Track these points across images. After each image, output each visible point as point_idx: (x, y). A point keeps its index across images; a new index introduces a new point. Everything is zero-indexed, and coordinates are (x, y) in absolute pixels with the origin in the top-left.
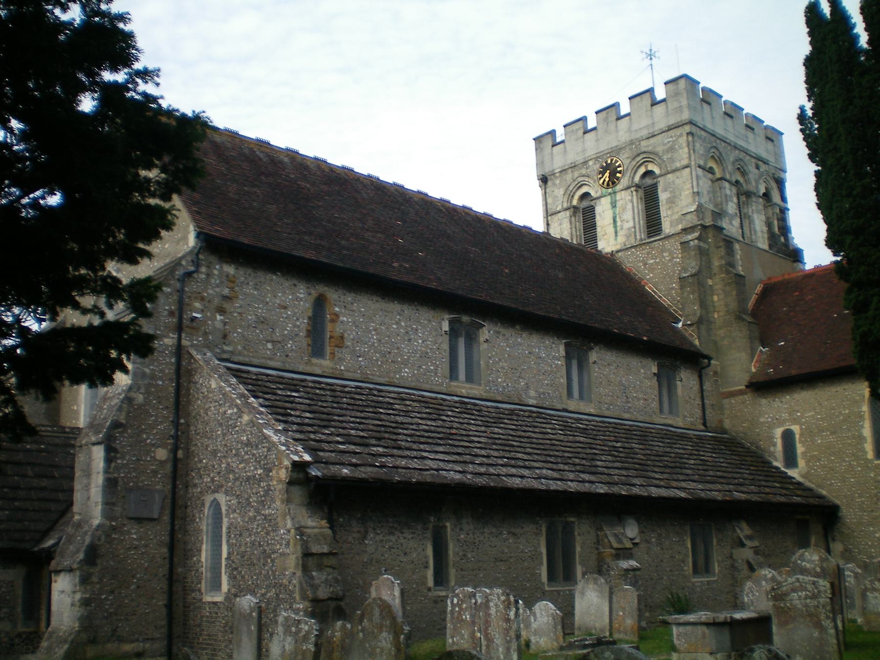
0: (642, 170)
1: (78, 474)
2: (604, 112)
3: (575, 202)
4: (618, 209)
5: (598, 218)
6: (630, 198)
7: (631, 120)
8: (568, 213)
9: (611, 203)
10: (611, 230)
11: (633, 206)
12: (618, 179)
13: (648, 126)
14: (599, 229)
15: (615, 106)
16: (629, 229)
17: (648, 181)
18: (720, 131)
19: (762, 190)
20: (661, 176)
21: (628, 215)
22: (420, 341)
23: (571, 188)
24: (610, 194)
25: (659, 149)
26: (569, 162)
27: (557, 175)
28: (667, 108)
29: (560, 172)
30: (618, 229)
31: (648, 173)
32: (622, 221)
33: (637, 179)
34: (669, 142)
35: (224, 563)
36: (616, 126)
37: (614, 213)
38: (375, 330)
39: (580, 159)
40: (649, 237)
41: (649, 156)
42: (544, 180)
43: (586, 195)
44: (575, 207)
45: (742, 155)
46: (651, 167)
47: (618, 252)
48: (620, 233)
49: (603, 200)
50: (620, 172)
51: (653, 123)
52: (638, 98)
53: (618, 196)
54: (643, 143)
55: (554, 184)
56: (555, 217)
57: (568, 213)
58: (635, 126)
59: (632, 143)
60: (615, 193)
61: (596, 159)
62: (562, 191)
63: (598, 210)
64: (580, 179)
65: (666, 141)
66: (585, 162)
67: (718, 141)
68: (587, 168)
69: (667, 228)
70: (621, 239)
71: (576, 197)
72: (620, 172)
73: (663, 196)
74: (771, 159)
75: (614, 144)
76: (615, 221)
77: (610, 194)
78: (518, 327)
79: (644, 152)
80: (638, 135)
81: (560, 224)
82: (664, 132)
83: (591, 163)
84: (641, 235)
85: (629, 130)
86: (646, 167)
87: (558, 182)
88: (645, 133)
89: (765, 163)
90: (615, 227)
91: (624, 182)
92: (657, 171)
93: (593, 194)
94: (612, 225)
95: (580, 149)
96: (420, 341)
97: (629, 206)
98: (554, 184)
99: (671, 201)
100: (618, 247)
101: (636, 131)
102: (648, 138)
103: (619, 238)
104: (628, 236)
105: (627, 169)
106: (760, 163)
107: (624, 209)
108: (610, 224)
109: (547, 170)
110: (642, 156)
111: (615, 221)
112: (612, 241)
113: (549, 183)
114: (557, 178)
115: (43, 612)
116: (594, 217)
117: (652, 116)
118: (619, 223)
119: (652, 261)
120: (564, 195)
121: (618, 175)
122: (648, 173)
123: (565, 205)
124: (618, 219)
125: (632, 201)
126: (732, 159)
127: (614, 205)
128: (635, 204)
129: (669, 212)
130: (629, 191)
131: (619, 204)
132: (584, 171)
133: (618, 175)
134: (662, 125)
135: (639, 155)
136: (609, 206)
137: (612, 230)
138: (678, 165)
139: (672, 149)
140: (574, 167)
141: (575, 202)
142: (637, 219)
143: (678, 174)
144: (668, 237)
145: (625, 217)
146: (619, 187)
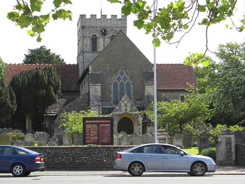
0: (112, 34)
8: (90, 39)
33: (110, 36)
39: (95, 26)
53: (105, 39)
54: (114, 28)
56: (86, 38)
57: (90, 39)
59: (111, 27)
66: (96, 27)
71: (92, 35)
83: (98, 28)
85: (110, 23)
87: (87, 29)
88: (115, 26)
91: (108, 36)
95: (95, 23)
98: (86, 29)
105: (109, 33)
109: (84, 25)
113: (84, 29)
114: (87, 28)
120: (89, 33)
127: (104, 41)
131: (106, 41)
132: (96, 29)
134: (120, 26)
140: (93, 27)
141: (91, 36)
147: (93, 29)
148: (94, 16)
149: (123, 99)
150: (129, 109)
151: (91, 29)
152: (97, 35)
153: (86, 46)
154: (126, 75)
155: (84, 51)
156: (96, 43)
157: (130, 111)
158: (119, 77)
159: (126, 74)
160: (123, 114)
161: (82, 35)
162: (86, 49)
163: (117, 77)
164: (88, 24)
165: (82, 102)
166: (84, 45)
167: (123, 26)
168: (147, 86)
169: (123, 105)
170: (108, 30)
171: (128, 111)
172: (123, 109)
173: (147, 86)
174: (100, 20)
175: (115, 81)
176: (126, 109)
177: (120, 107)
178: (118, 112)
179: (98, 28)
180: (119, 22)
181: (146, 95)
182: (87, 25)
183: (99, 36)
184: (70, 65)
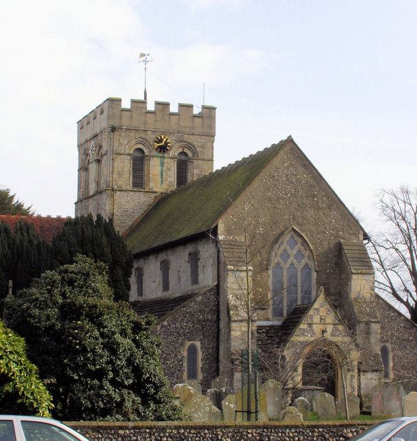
0: (181, 150)
3: (131, 152)
7: (179, 118)
8: (129, 157)
15: (167, 105)
17: (183, 158)
24: (161, 157)
25: (195, 143)
31: (183, 153)
33: (176, 154)
37: (162, 169)
41: (190, 146)
46: (186, 150)
49: (155, 159)
52: (185, 108)
53: (166, 160)
56: (120, 157)
58: (182, 124)
59: (179, 132)
60: (164, 157)
72: (169, 146)
76: (162, 175)
81: (123, 162)
83: (149, 133)
87: (123, 134)
88: (187, 130)
90: (162, 178)
91: (171, 153)
92: (190, 154)
98: (120, 135)
111: (162, 175)
112: (159, 186)
122: (183, 153)
127: (162, 165)
134: (198, 130)
136: (159, 164)
137: (160, 179)
141: (131, 152)
146: (166, 155)
147: (138, 136)
148: (140, 105)
149: (316, 306)
150: (330, 329)
152: (146, 151)
153: (120, 175)
154: (302, 248)
155: (115, 187)
156: (142, 170)
157: (333, 335)
158: (285, 250)
159: (302, 245)
160: (317, 342)
161: (112, 147)
162: (120, 183)
163: (280, 252)
164: (125, 123)
165: (200, 311)
166: (115, 172)
168: (354, 277)
169: (316, 319)
171: (328, 335)
172: (317, 328)
173: (354, 277)
174: (153, 115)
175: (276, 262)
176: (323, 332)
177: (310, 325)
178: (304, 335)
179: (149, 133)
180: (198, 121)
181: (352, 297)
182: (123, 124)
183: (150, 152)
184: (49, 217)
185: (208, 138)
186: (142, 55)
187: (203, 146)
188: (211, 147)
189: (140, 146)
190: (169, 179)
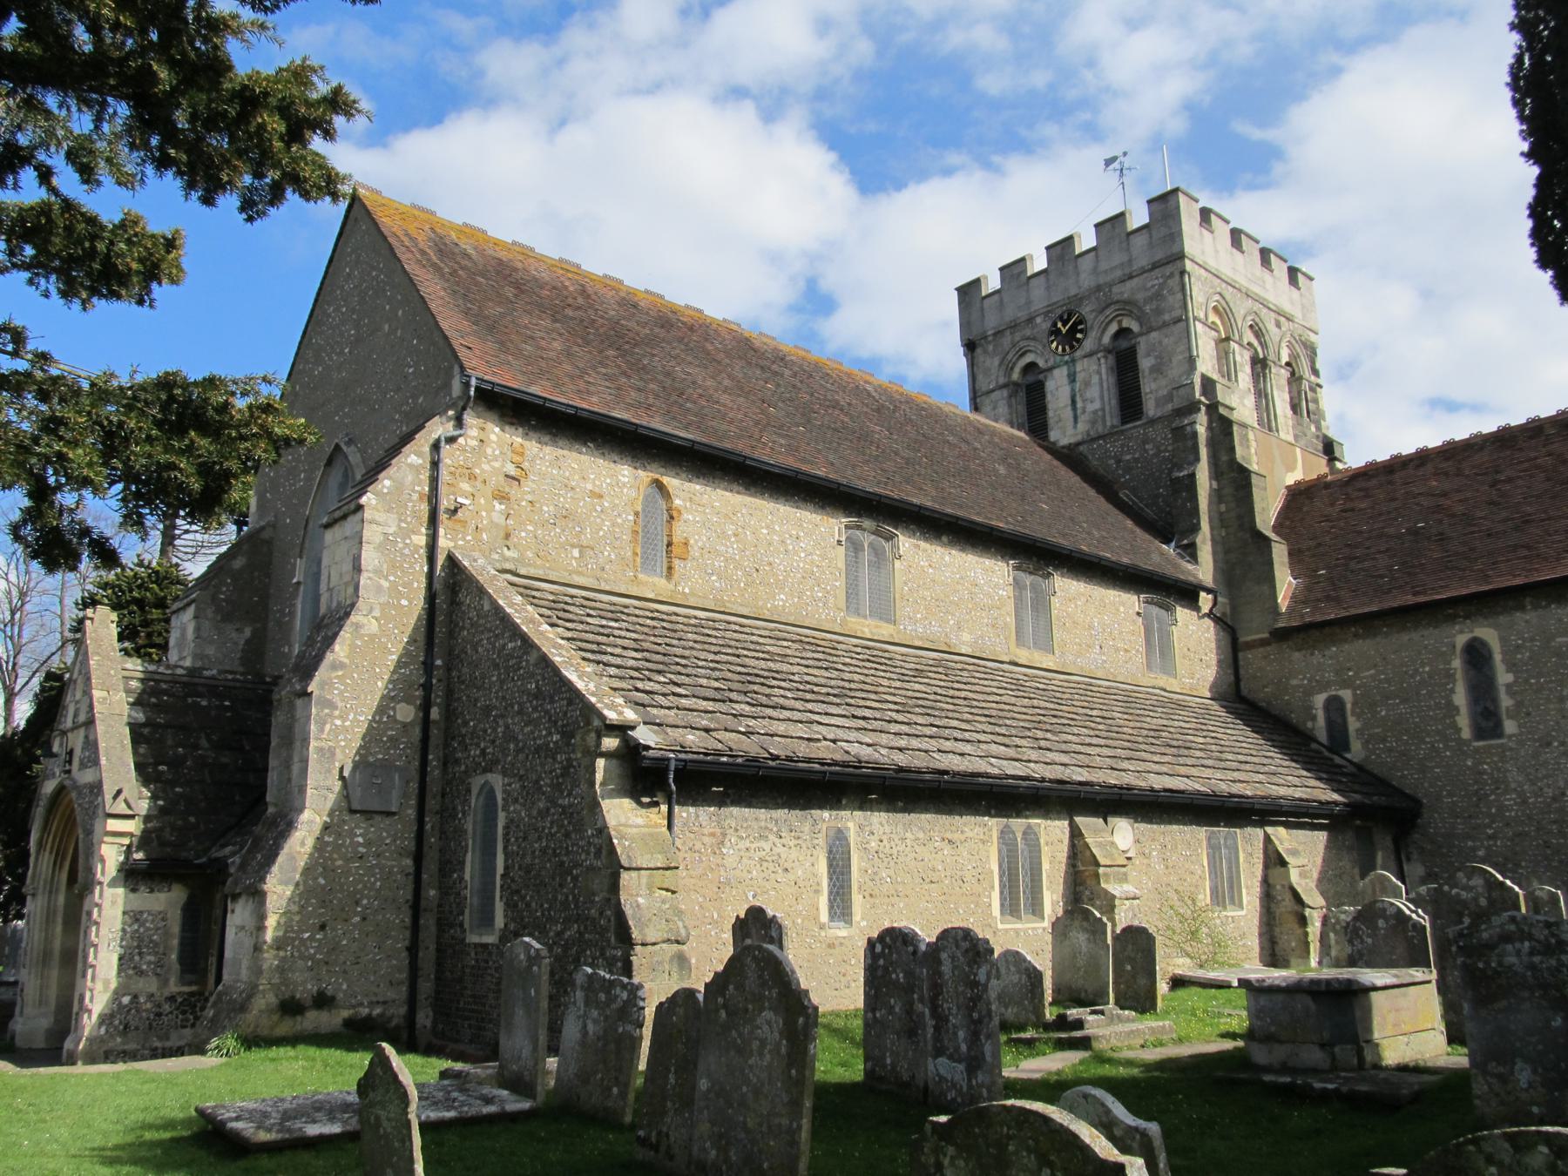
0: (1114, 328)
1: (274, 742)
2: (1059, 247)
4: (1078, 385)
5: (1049, 397)
6: (1095, 367)
7: (1097, 256)
8: (1005, 393)
9: (1069, 375)
10: (1069, 413)
11: (1101, 379)
12: (1078, 341)
13: (1122, 264)
14: (1051, 414)
16: (1095, 412)
17: (1124, 344)
18: (1226, 271)
19: (1285, 358)
20: (1141, 334)
21: (1093, 392)
22: (803, 555)
23: (1009, 357)
25: (1140, 296)
26: (1007, 319)
27: (990, 338)
28: (1151, 237)
29: (995, 334)
30: (1079, 412)
31: (1122, 333)
32: (1084, 401)
33: (1106, 339)
34: (1153, 286)
35: (498, 882)
36: (1076, 267)
37: (1073, 390)
38: (736, 535)
39: (1023, 315)
40: (1124, 423)
41: (1128, 307)
42: (970, 346)
43: (1031, 367)
44: (1016, 384)
45: (1257, 307)
46: (1125, 324)
47: (1078, 444)
48: (1082, 418)
49: (1056, 372)
50: (1081, 331)
51: (1130, 261)
53: (1079, 367)
55: (985, 352)
57: (1005, 393)
58: (1104, 266)
59: (1099, 288)
60: (1073, 361)
61: (1046, 314)
62: (996, 361)
63: (1050, 385)
64: (1022, 344)
65: (1149, 285)
66: (1031, 320)
67: (1224, 285)
68: (1033, 328)
69: (1151, 408)
70: (1082, 427)
71: (1017, 370)
73: (1145, 363)
74: (1297, 313)
75: (1073, 292)
76: (1074, 402)
77: (1067, 363)
78: (944, 539)
79: (1117, 302)
80: (1108, 279)
81: (994, 408)
82: (1145, 272)
83: (1039, 320)
84: (1112, 420)
85: (1095, 271)
86: (1120, 322)
87: (991, 348)
88: (1118, 273)
89: (1288, 319)
91: (1088, 345)
93: (1041, 363)
94: (1069, 408)
95: (1023, 301)
96: (803, 555)
97: (1095, 379)
98: (985, 352)
99: (1157, 370)
100: (1079, 438)
101: (1106, 272)
102: (1123, 281)
103: (1079, 425)
104: (1093, 422)
105: (1092, 327)
106: (1282, 319)
107: (1087, 384)
108: (1066, 406)
109: (975, 333)
110: (1113, 307)
111: (1074, 402)
112: (1070, 431)
113: (979, 351)
114: (990, 342)
115: (213, 960)
116: (1043, 396)
117: (1128, 250)
118: (1079, 405)
119: (1128, 457)
120: (1000, 365)
121: (1079, 336)
122: (1122, 333)
123: (1002, 380)
124: (1078, 399)
125: (1099, 373)
126: (1242, 312)
127: (1072, 378)
128: (1104, 377)
129: (1153, 386)
130: (1095, 358)
131: (1079, 377)
132: (1028, 332)
133: (1079, 336)
134: (1143, 262)
135: (1108, 306)
136: (1065, 381)
138: (1167, 317)
139: (1158, 296)
140: (1014, 326)
141: (1016, 376)
142: (1106, 399)
143: (1165, 331)
144: (1152, 422)
145: (1088, 395)
146: (1078, 354)
151: (1007, 340)
167: (1159, 255)
170: (1087, 310)
185: (1168, 270)
186: (1109, 162)
187: (1158, 296)
188: (1177, 288)
189: (1029, 358)
190: (1091, 407)
